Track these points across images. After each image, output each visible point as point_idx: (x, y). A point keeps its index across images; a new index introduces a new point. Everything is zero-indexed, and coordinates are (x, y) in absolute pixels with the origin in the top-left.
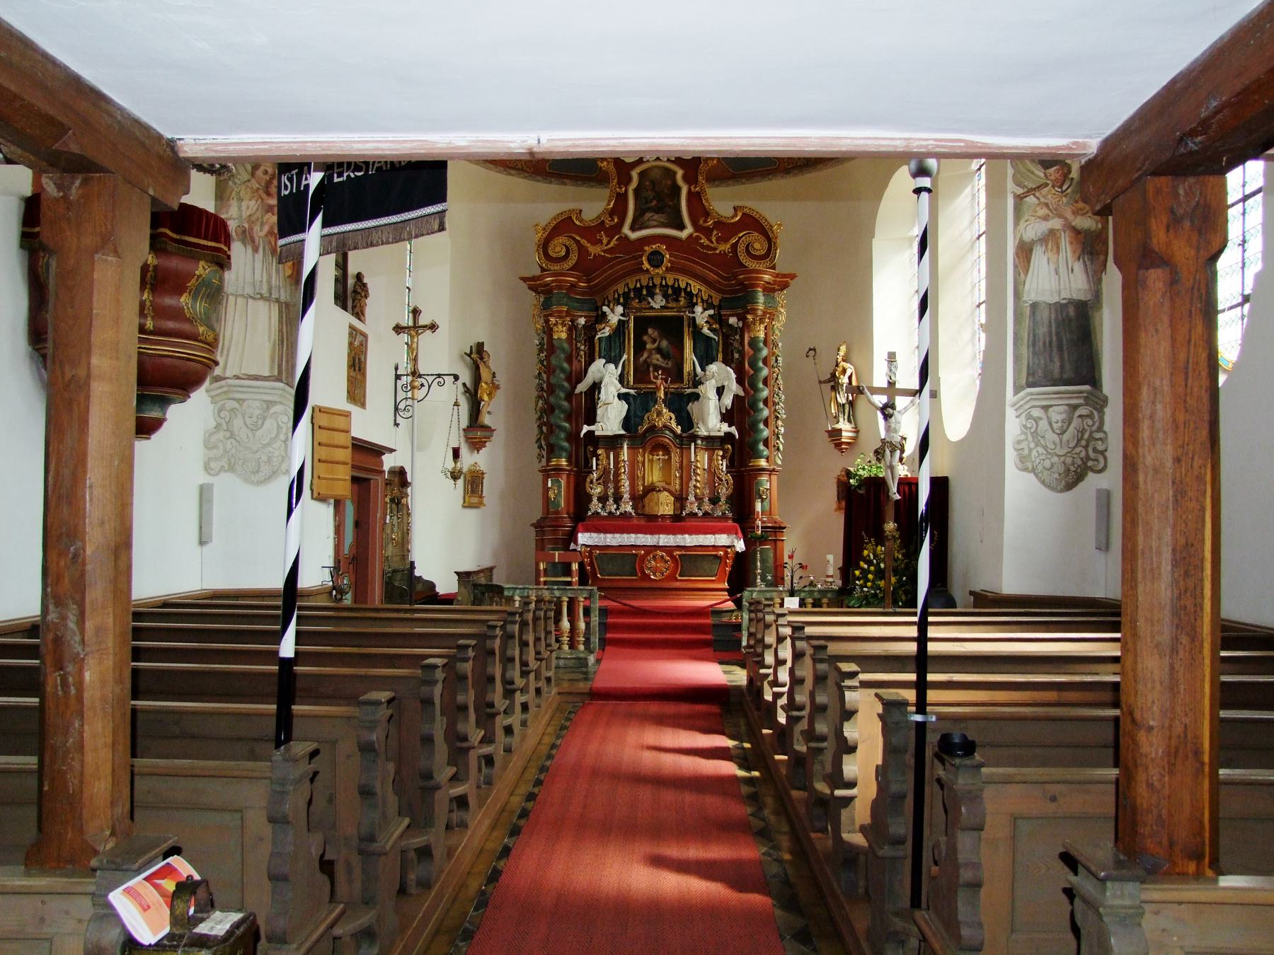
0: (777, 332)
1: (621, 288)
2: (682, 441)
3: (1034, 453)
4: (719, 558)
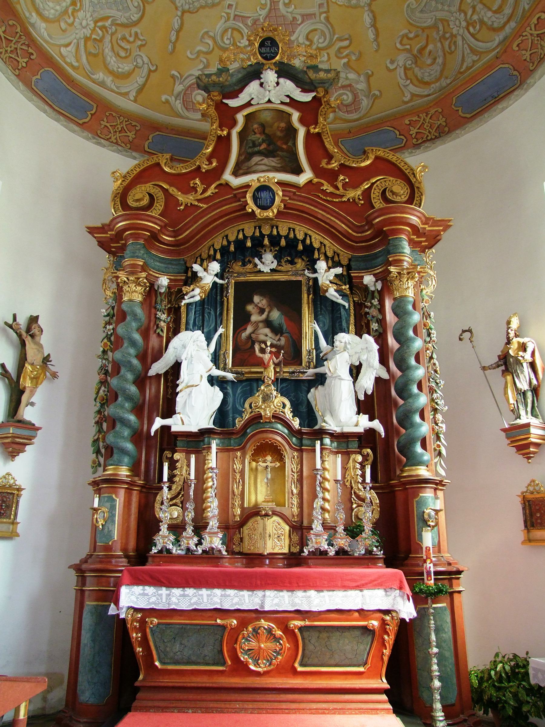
1: (218, 242)
2: (301, 440)
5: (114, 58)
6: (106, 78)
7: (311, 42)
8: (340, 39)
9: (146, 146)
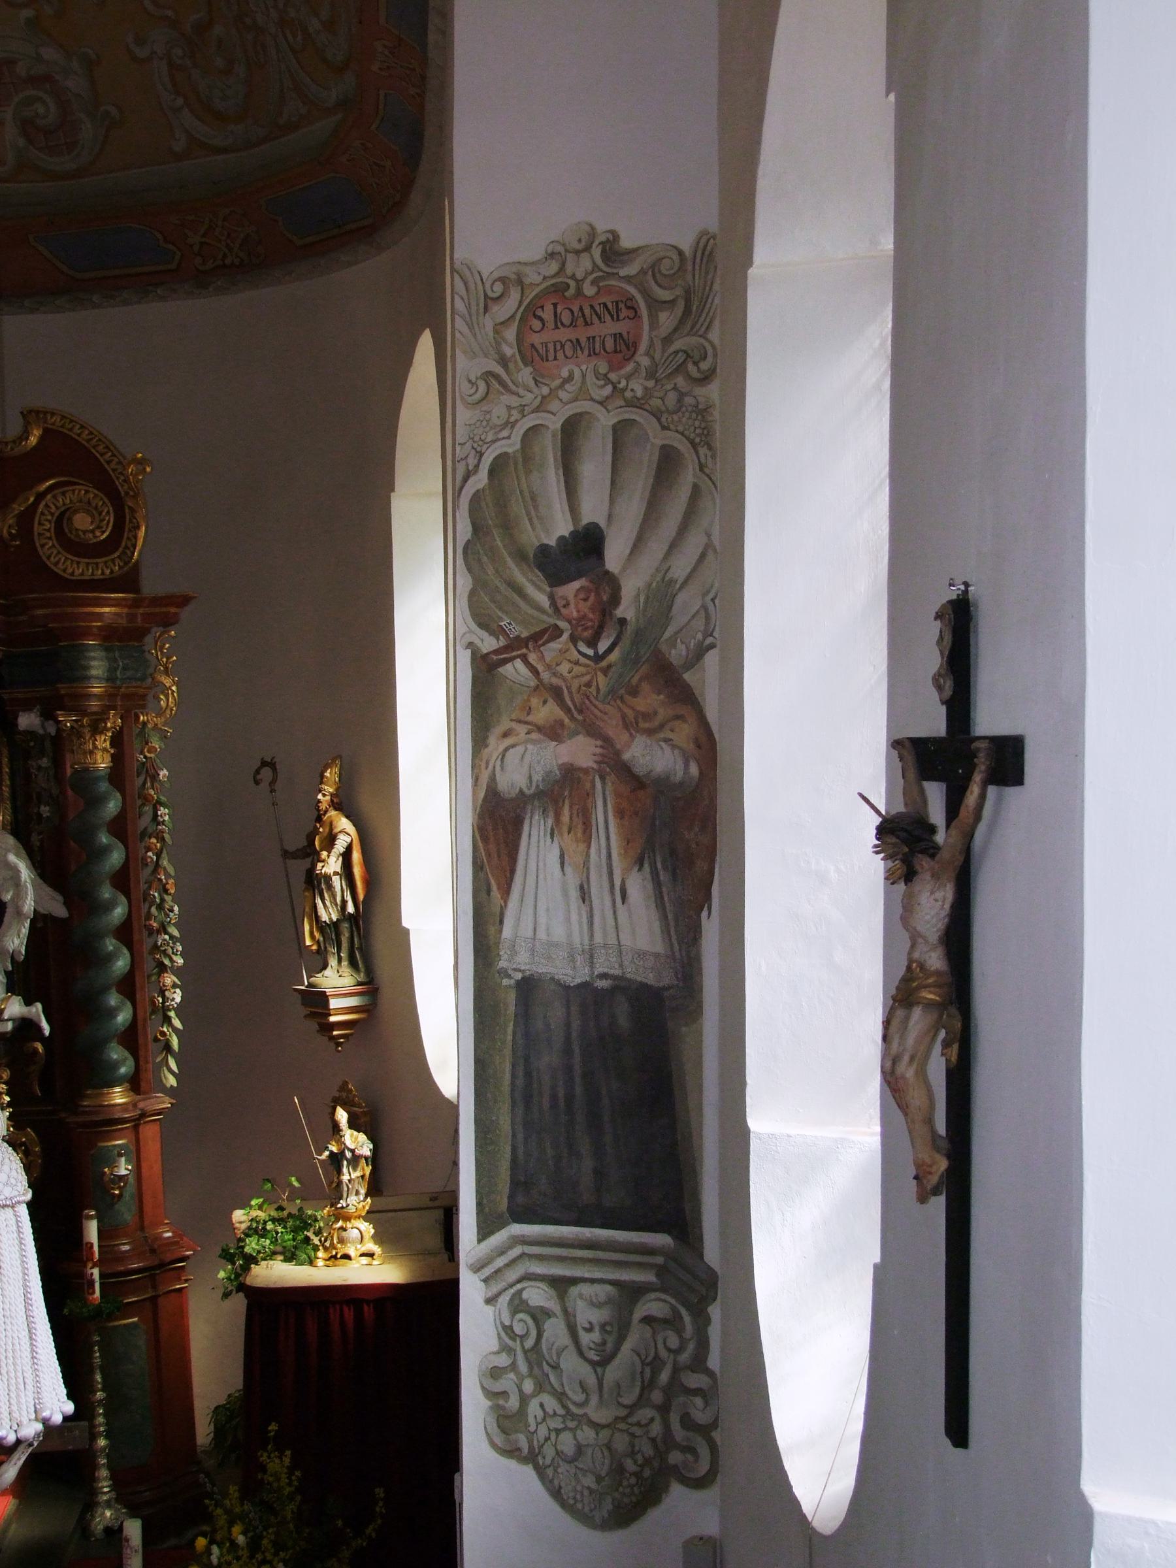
0: (156, 743)
3: (533, 1408)
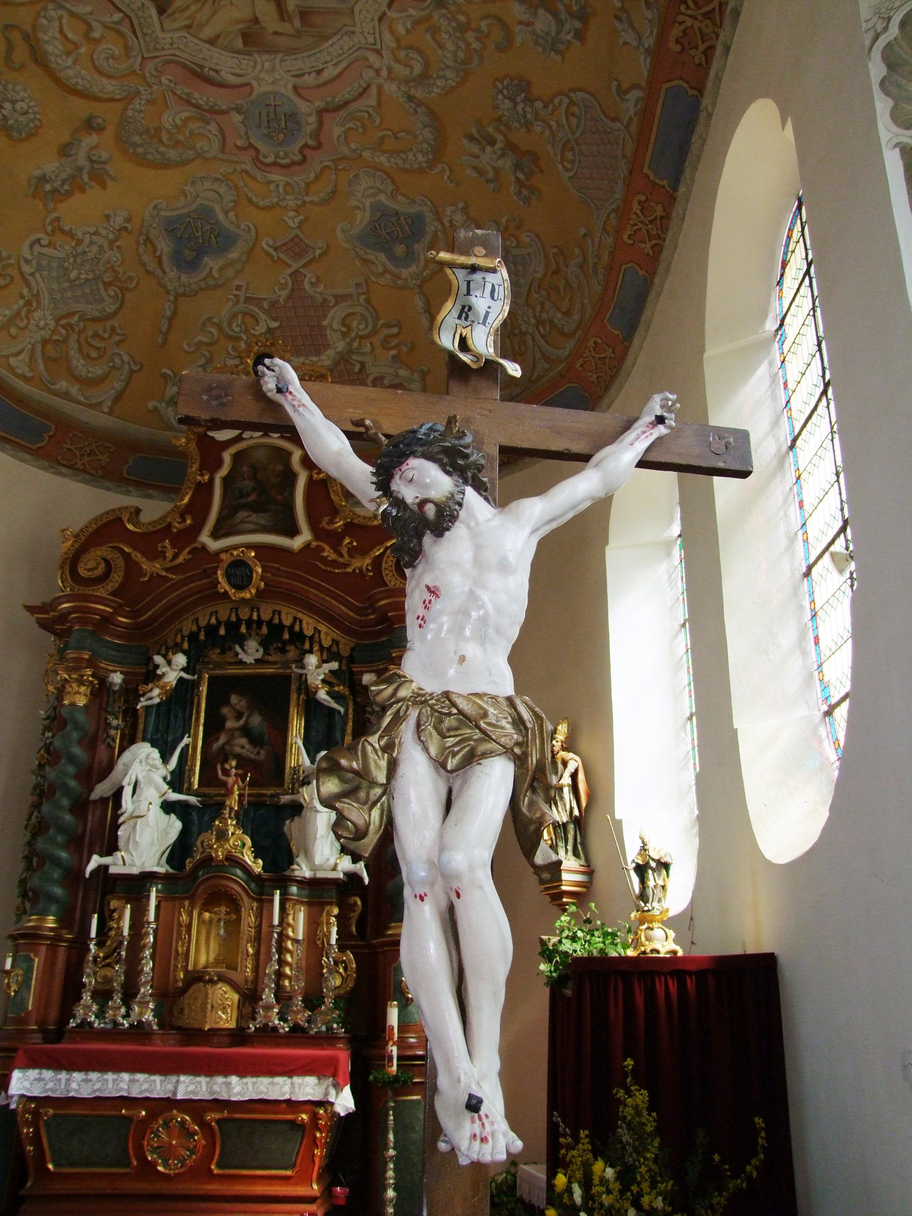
1: (188, 627)
4: (301, 1126)
5: (82, 362)
6: (70, 389)
7: (349, 328)
8: (388, 326)
9: (125, 472)
